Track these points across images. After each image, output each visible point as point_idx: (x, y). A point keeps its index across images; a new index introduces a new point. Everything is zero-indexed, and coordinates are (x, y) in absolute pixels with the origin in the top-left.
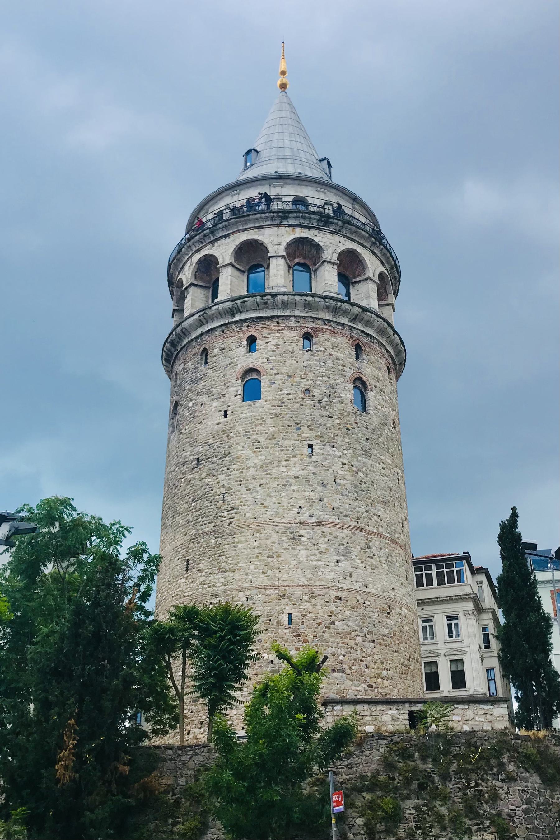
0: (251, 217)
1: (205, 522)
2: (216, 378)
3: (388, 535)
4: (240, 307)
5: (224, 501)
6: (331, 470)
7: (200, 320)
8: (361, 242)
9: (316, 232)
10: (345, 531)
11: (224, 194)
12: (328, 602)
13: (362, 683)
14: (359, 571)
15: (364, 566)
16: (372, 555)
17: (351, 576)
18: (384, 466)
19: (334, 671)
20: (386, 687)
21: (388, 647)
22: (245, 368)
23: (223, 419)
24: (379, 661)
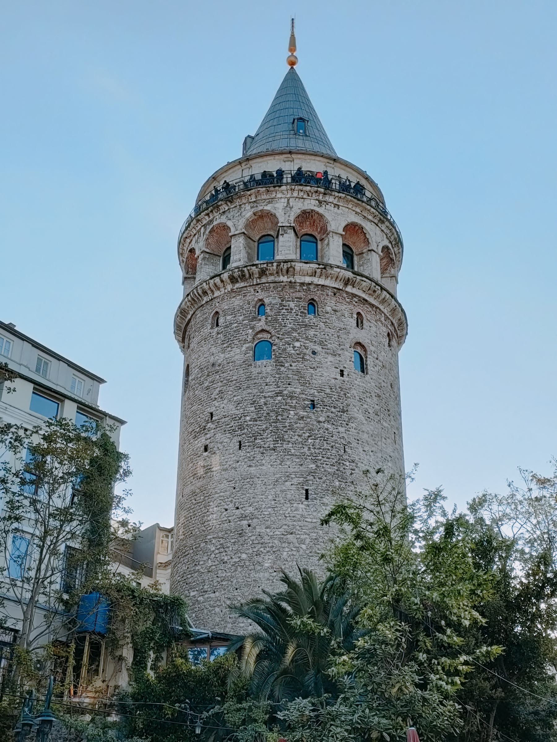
0: (363, 204)
1: (327, 463)
2: (330, 335)
4: (357, 282)
5: (345, 451)
7: (315, 272)
11: (318, 158)
22: (358, 341)
23: (338, 376)
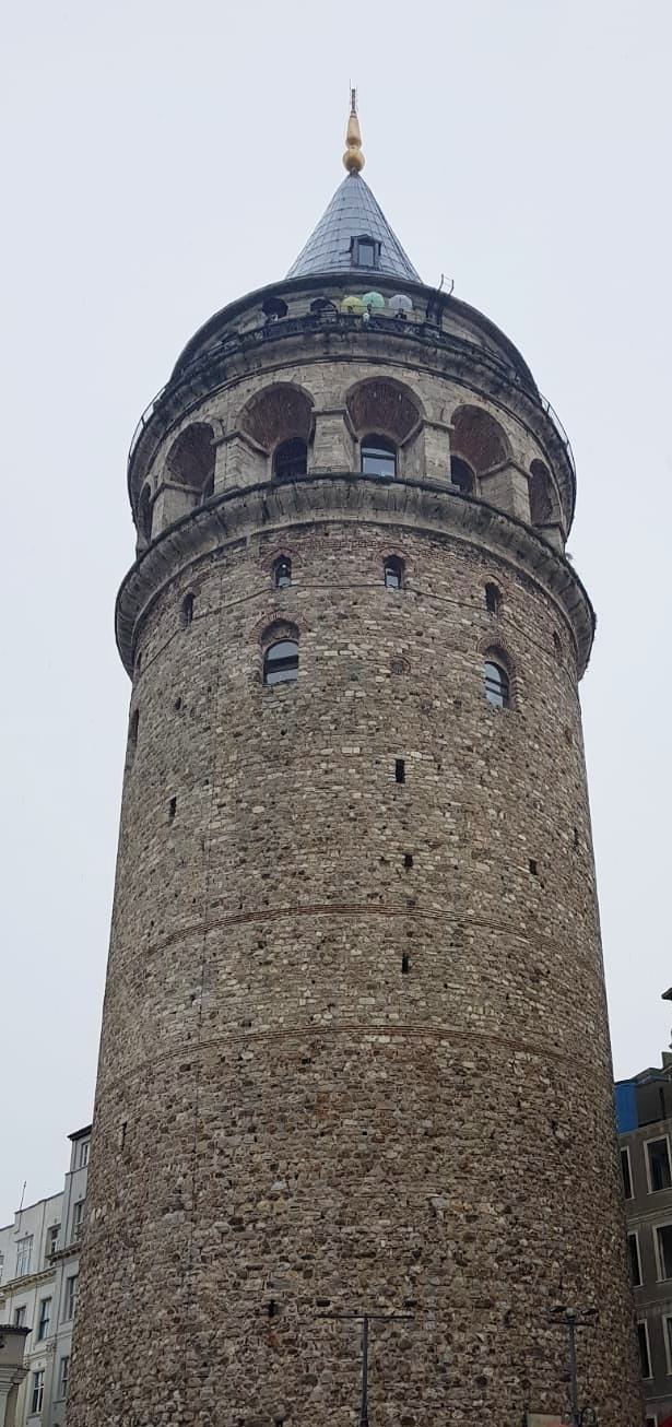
3: (327, 902)
6: (197, 831)
8: (296, 358)
9: (208, 404)
10: (212, 934)
12: (168, 1082)
13: (215, 1218)
14: (231, 1000)
15: (245, 985)
16: (270, 957)
17: (212, 1016)
18: (331, 766)
19: (166, 1211)
20: (279, 1214)
21: (297, 1131)
24: (265, 1166)
